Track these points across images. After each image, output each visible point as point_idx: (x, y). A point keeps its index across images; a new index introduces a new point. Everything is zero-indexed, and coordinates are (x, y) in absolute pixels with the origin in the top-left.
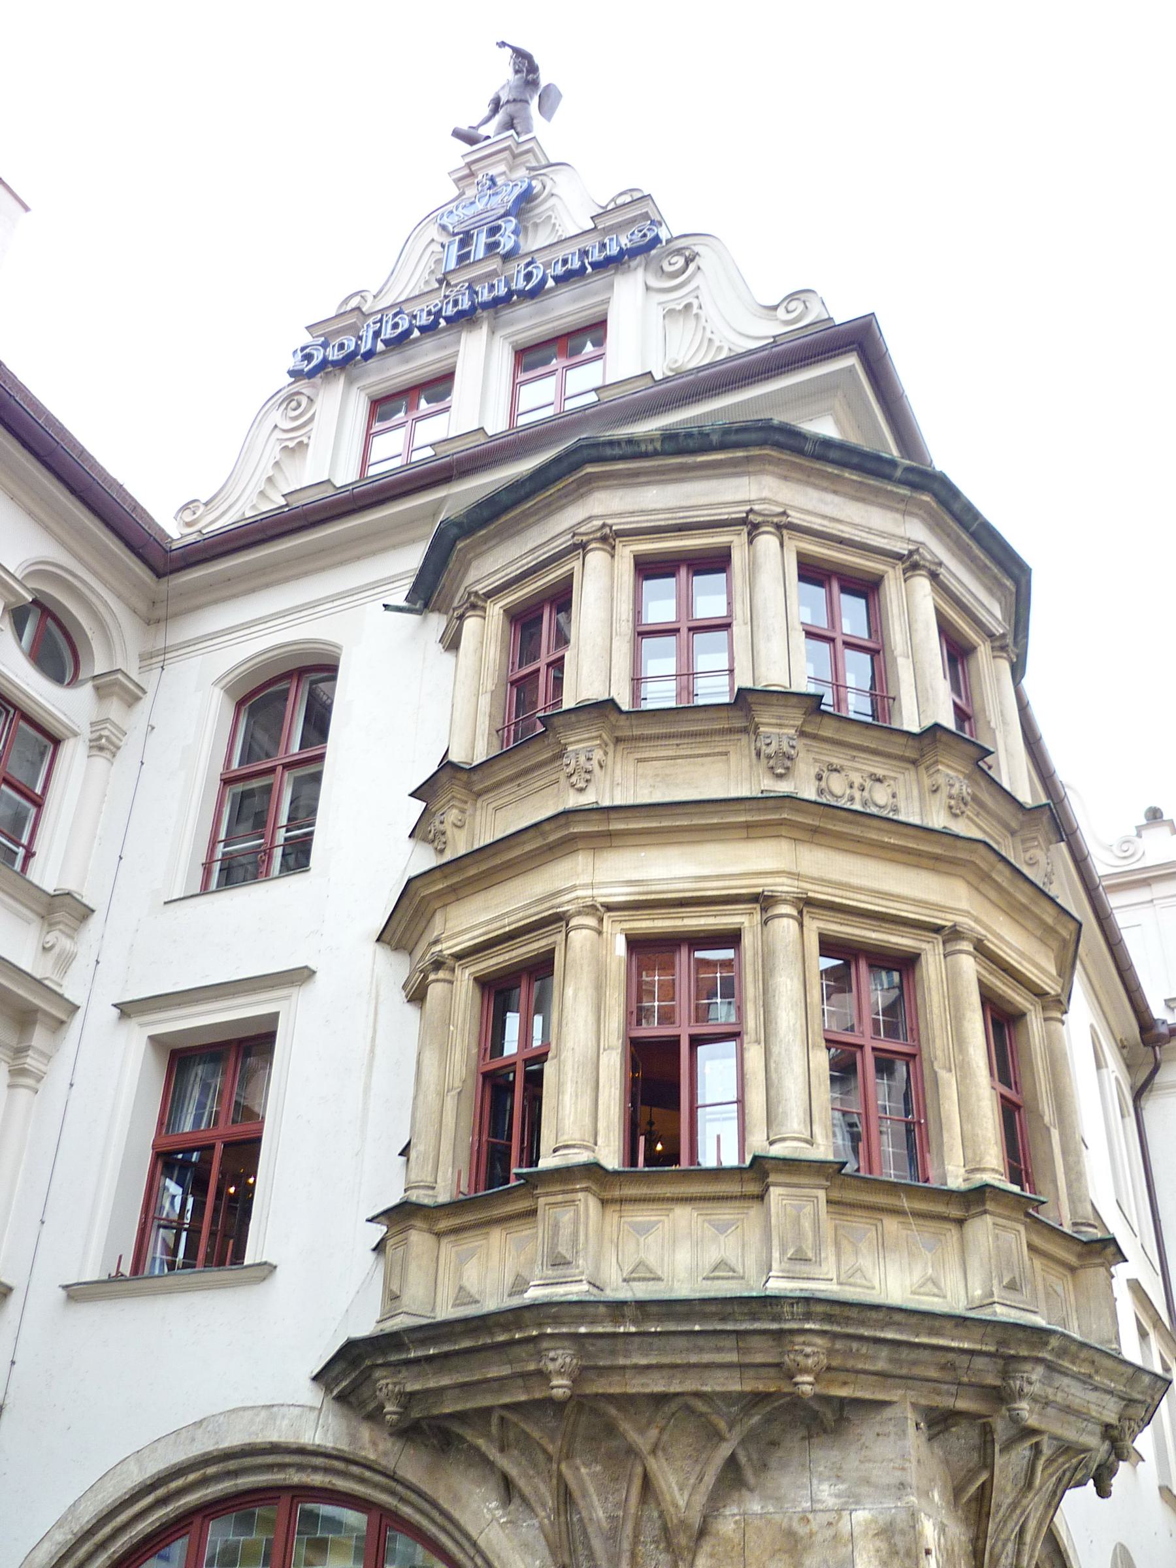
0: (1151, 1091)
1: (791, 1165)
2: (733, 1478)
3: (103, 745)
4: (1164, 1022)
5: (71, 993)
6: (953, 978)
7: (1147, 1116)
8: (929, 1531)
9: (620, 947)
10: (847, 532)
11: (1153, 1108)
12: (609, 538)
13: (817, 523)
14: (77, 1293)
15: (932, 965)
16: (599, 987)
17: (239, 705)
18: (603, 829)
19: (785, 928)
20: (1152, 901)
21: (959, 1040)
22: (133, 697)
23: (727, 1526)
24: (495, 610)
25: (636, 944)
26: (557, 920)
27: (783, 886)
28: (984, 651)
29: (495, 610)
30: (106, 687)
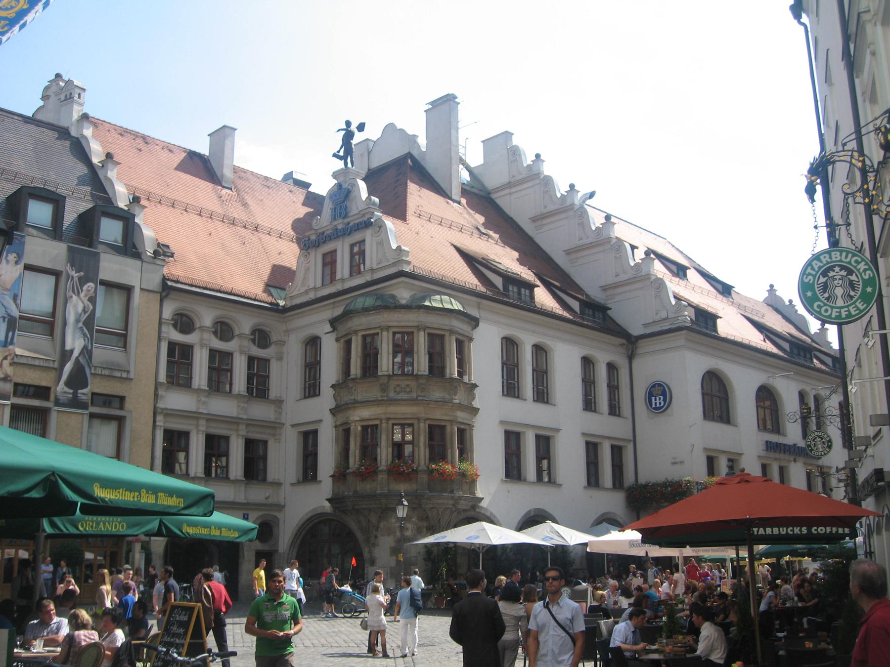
1: (381, 471)
2: (380, 519)
3: (280, 359)
5: (283, 421)
6: (419, 427)
8: (409, 526)
9: (359, 428)
10: (403, 324)
11: (635, 363)
12: (356, 332)
13: (396, 324)
14: (292, 484)
15: (416, 427)
16: (355, 437)
17: (306, 345)
18: (356, 404)
19: (384, 425)
21: (419, 440)
22: (282, 343)
23: (382, 525)
24: (342, 341)
25: (363, 427)
26: (347, 423)
27: (383, 416)
28: (447, 334)
29: (342, 341)
30: (276, 343)
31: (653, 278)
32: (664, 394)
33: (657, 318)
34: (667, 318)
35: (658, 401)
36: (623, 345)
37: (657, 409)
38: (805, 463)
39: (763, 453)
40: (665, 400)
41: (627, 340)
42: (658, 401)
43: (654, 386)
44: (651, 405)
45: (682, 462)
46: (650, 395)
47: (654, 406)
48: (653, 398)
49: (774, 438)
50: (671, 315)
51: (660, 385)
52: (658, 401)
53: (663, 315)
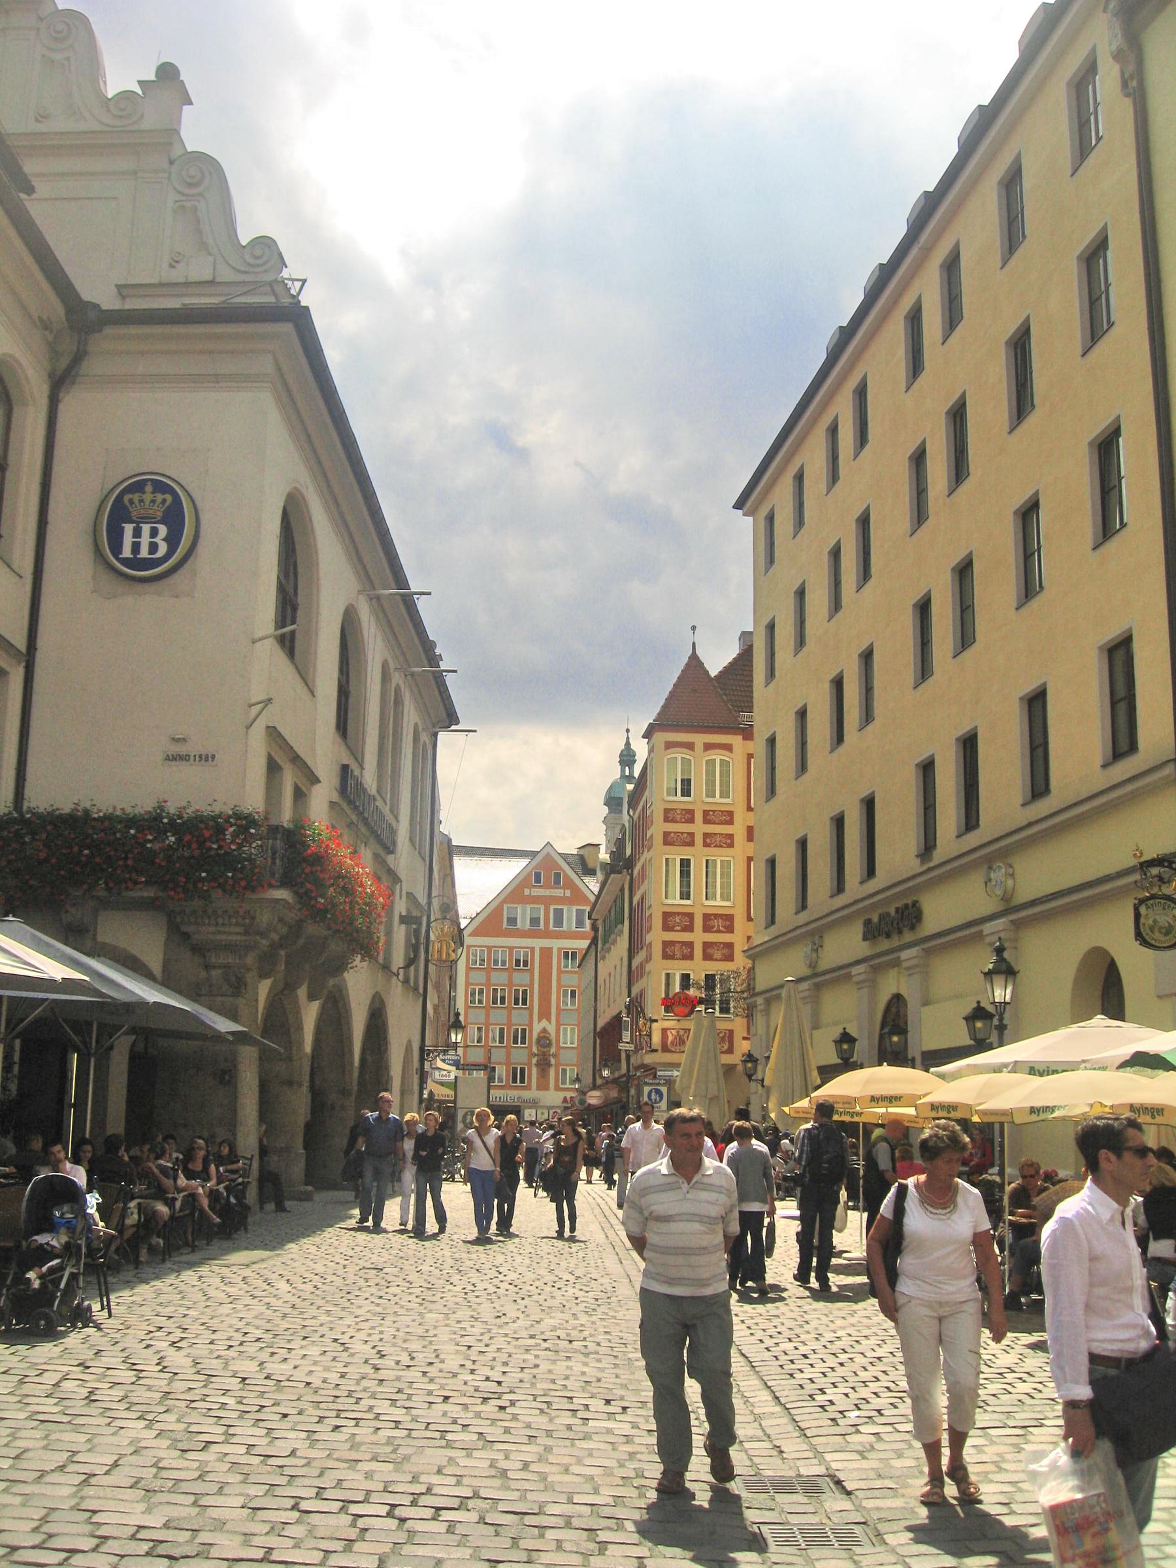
0: (73, 383)
4: (95, 306)
7: (61, 407)
11: (72, 404)
20: (135, 173)
31: (177, 152)
32: (174, 518)
33: (177, 275)
34: (212, 283)
35: (145, 540)
36: (46, 326)
37: (136, 563)
38: (376, 856)
39: (335, 797)
40: (173, 541)
41: (69, 311)
42: (144, 539)
43: (138, 487)
44: (116, 548)
45: (206, 758)
46: (118, 513)
47: (127, 553)
48: (129, 529)
49: (354, 766)
50: (226, 275)
51: (160, 487)
52: (145, 540)
53: (198, 269)
